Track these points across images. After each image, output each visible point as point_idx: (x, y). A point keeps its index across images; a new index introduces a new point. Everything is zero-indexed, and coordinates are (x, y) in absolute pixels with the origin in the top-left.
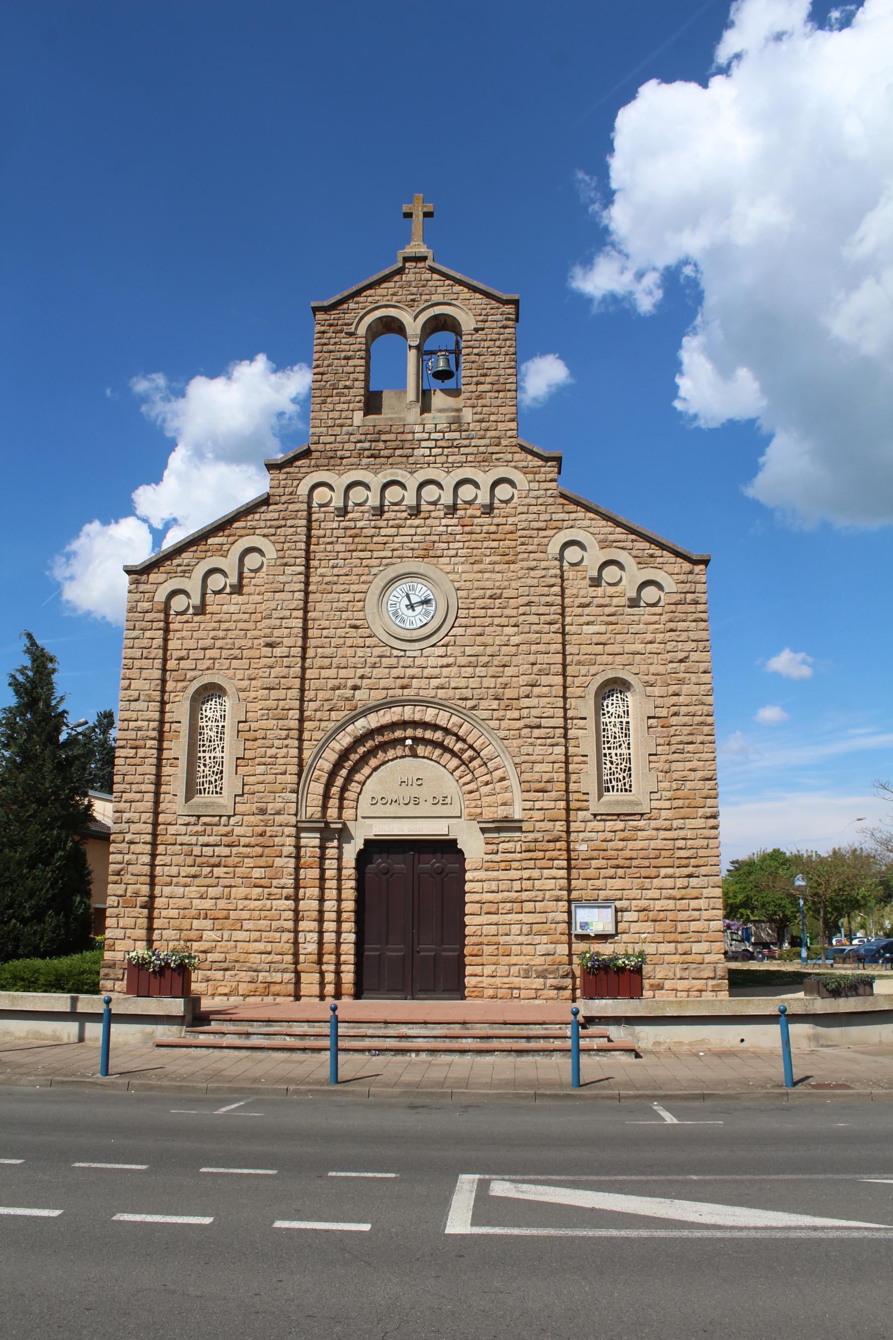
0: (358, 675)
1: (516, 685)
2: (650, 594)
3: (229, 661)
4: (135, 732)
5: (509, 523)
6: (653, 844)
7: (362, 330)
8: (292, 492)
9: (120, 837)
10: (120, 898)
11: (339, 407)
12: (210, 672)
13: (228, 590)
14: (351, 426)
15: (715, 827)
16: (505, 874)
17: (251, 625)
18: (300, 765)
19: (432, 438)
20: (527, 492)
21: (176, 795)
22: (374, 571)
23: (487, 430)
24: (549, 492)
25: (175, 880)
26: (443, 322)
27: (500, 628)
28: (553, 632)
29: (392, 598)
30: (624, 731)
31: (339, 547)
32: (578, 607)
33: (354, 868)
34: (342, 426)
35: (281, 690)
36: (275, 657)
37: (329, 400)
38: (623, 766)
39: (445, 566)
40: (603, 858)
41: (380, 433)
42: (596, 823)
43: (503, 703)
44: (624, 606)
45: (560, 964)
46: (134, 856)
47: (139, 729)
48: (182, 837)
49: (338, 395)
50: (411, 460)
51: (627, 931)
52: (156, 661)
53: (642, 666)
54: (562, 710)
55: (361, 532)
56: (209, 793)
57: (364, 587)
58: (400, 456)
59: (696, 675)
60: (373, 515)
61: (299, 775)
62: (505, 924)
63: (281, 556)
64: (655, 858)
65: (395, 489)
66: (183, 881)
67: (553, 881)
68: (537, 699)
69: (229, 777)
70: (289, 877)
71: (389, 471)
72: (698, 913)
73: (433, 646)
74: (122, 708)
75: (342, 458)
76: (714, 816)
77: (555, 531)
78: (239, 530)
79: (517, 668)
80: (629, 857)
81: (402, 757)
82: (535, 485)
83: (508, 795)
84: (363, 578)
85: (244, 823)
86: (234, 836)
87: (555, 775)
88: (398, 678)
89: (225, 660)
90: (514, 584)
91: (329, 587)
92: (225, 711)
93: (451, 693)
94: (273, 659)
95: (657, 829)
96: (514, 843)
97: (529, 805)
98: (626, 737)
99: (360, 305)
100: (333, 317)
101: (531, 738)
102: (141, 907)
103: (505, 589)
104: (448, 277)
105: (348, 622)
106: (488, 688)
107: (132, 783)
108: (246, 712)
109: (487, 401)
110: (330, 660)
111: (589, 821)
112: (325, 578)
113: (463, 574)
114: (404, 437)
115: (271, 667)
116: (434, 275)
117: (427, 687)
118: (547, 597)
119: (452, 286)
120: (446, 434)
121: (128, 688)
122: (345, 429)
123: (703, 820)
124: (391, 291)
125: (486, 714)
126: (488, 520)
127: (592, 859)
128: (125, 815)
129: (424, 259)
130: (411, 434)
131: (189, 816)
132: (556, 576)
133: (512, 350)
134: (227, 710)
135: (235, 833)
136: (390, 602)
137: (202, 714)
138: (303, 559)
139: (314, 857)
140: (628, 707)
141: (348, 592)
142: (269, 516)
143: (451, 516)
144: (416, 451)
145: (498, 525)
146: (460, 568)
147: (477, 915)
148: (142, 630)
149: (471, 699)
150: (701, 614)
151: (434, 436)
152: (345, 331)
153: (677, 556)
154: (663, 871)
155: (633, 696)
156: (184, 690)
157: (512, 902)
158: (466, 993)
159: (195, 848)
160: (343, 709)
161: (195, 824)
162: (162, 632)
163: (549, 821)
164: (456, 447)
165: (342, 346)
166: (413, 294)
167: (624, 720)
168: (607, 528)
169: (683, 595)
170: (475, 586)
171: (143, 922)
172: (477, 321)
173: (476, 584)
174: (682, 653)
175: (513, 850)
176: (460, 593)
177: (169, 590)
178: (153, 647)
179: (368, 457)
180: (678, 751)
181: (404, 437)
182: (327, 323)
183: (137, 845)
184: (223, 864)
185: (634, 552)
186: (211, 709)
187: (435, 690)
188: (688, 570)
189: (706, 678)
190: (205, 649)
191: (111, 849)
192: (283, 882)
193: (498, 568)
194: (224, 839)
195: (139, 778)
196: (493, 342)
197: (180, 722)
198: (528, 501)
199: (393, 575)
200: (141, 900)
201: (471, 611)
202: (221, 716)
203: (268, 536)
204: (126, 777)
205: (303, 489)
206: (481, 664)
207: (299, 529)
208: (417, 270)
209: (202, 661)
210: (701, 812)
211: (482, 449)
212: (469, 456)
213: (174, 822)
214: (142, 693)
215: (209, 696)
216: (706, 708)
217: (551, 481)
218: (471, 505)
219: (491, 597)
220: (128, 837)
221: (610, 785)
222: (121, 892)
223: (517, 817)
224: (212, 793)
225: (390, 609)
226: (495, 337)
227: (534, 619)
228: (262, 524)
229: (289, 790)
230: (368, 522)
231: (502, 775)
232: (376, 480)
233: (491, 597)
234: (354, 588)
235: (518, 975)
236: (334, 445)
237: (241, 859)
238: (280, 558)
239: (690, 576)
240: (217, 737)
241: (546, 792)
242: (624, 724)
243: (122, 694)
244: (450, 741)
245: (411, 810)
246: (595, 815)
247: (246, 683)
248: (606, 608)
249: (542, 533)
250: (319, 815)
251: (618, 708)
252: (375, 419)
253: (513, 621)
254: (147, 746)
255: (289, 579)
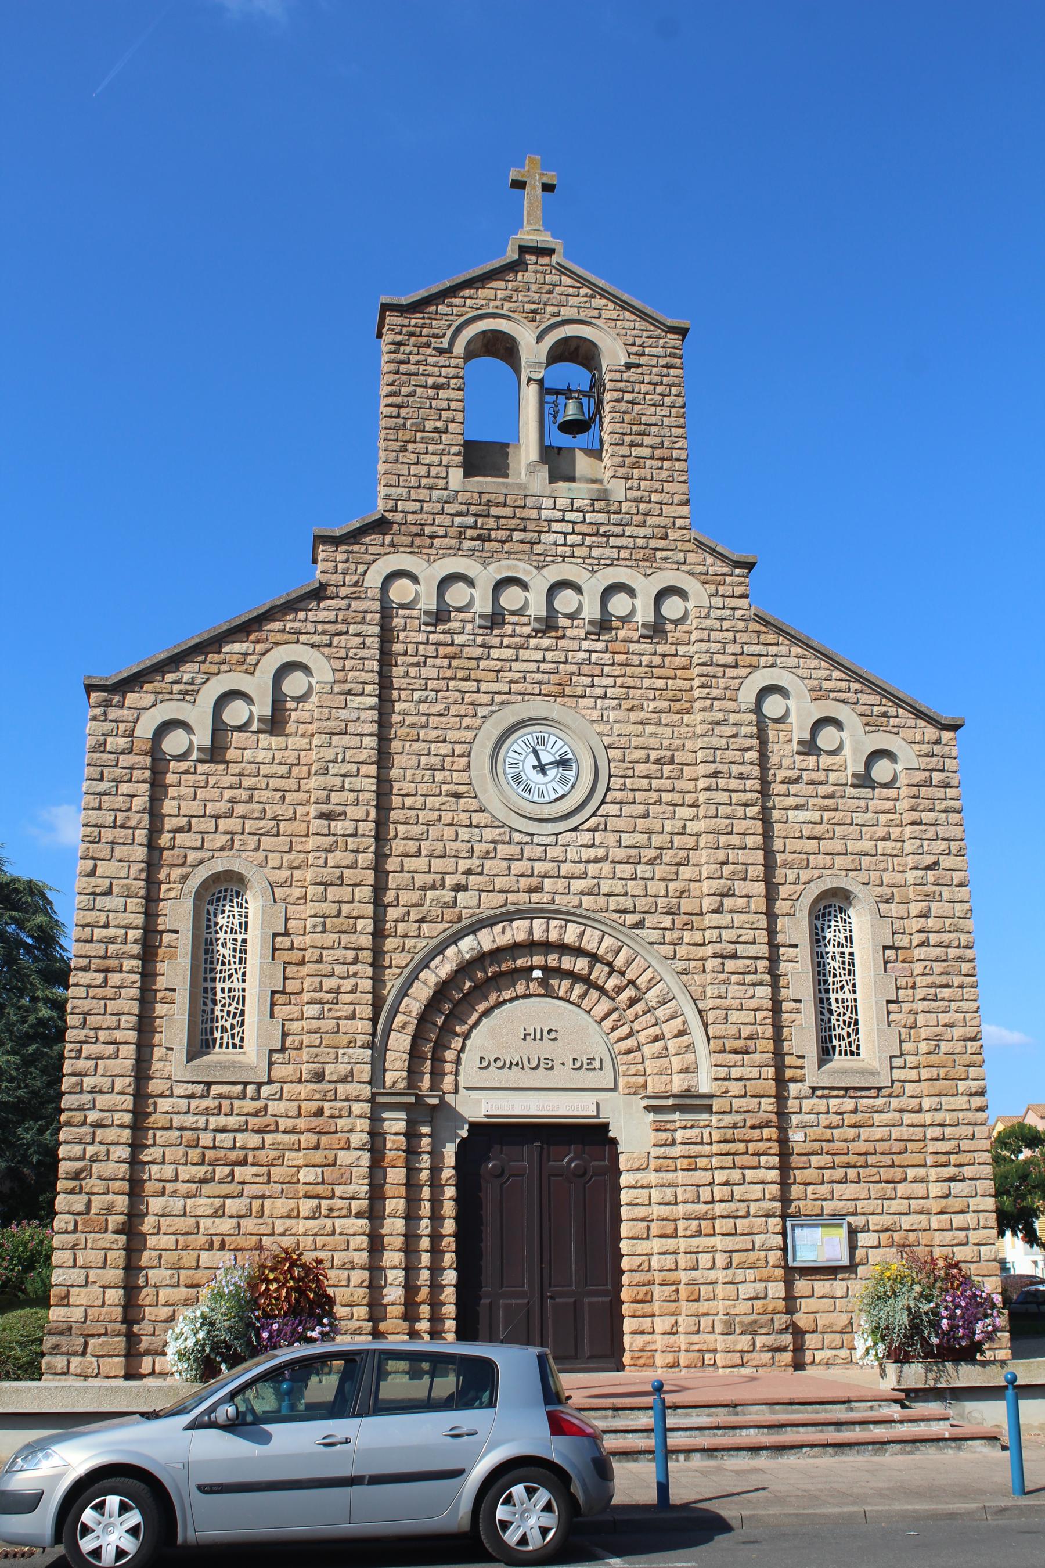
0: (461, 869)
1: (698, 893)
2: (882, 770)
3: (257, 837)
4: (103, 946)
5: (680, 653)
6: (896, 1132)
7: (459, 348)
8: (357, 582)
9: (78, 1117)
10: (78, 1218)
11: (427, 459)
12: (226, 853)
13: (255, 727)
14: (446, 489)
15: (981, 1109)
16: (688, 1176)
17: (292, 784)
18: (377, 1005)
19: (567, 518)
20: (706, 610)
21: (171, 1049)
22: (482, 711)
23: (647, 514)
24: (738, 614)
25: (169, 1187)
26: (572, 348)
27: (671, 808)
28: (750, 818)
29: (511, 754)
30: (847, 967)
31: (426, 672)
32: (782, 782)
33: (454, 1168)
34: (431, 488)
35: (345, 887)
36: (335, 835)
37: (410, 447)
38: (846, 1018)
39: (589, 711)
40: (827, 1153)
41: (488, 503)
42: (815, 1100)
43: (679, 921)
44: (846, 785)
45: (775, 1312)
46: (103, 1149)
47: (112, 940)
48: (182, 1117)
49: (423, 440)
50: (538, 549)
51: (864, 1261)
52: (137, 832)
53: (871, 873)
54: (765, 932)
55: (461, 651)
56: (221, 1046)
57: (469, 735)
58: (522, 542)
59: (950, 888)
60: (480, 627)
61: (375, 1020)
62: (690, 1253)
63: (341, 679)
64: (900, 1153)
65: (514, 590)
66: (182, 1188)
67: (760, 1186)
68: (729, 916)
69: (259, 1021)
70: (361, 1182)
71: (504, 562)
72: (964, 1233)
73: (575, 829)
74: (81, 906)
75: (432, 537)
76: (981, 1093)
77: (749, 670)
78: (273, 634)
79: (697, 869)
80: (863, 1151)
81: (525, 996)
82: (717, 601)
83: (689, 1058)
84: (466, 722)
85: (285, 1095)
86: (268, 1116)
87: (760, 1029)
88: (522, 876)
89: (251, 837)
90: (689, 745)
91: (414, 732)
92: (246, 917)
93: (602, 900)
94: (331, 839)
95: (901, 1111)
96: (699, 1130)
97: (722, 1072)
98: (849, 975)
99: (455, 309)
100: (413, 322)
101: (723, 972)
102: (115, 1232)
103: (677, 750)
104: (585, 282)
105: (445, 788)
106: (655, 896)
107: (99, 1028)
108: (287, 920)
109: (646, 472)
110: (417, 843)
111: (806, 1098)
112: (406, 717)
113: (616, 726)
114: (527, 513)
115: (327, 851)
116: (564, 278)
117: (566, 891)
118: (740, 766)
119: (592, 296)
120: (588, 516)
121: (93, 873)
122: (436, 494)
123: (966, 1098)
124: (500, 294)
125: (655, 936)
126: (649, 648)
127: (813, 1154)
128: (86, 1079)
129: (550, 252)
130: (536, 511)
131: (193, 1082)
132: (751, 737)
133: (680, 401)
134: (250, 915)
135: (269, 1113)
136: (508, 760)
137: (209, 920)
138: (376, 686)
139: (397, 1149)
140: (851, 931)
141: (444, 741)
142: (322, 616)
143: (596, 637)
144: (543, 536)
145: (664, 656)
146: (613, 716)
147: (642, 1239)
148: (114, 780)
149: (634, 912)
150: (953, 802)
151: (569, 516)
152: (433, 345)
153: (918, 717)
154: (911, 1173)
155: (859, 915)
156: (185, 878)
157: (699, 1219)
158: (626, 1359)
159: (202, 1135)
160: (440, 919)
161: (202, 1097)
162: (148, 786)
163: (752, 1096)
164: (602, 535)
165: (429, 368)
166: (534, 303)
167: (847, 951)
168: (818, 668)
169: (927, 774)
170: (633, 744)
171: (117, 1256)
172: (629, 354)
173: (635, 741)
174: (929, 856)
175: (699, 1140)
176: (613, 753)
177: (159, 720)
178: (134, 809)
179: (473, 539)
180: (929, 997)
181: (527, 513)
182: (405, 330)
183: (108, 1130)
184: (250, 1159)
185: (860, 709)
186: (223, 912)
187: (578, 897)
188: (934, 738)
189: (962, 893)
190: (217, 817)
191: (62, 1137)
192: (351, 1189)
193: (665, 718)
194: (254, 1121)
195: (111, 1021)
196: (652, 387)
197: (177, 932)
198: (708, 623)
199: (513, 720)
200: (114, 1221)
201: (628, 780)
202: (240, 923)
203: (319, 646)
204: (88, 1017)
205: (374, 578)
206: (645, 860)
207: (369, 641)
208: (540, 268)
209: (211, 836)
210: (962, 1086)
211: (640, 542)
212: (622, 551)
213: (168, 1093)
214: (115, 882)
215: (220, 892)
216: (963, 938)
217: (741, 596)
218: (624, 622)
219: (657, 762)
220: (92, 1117)
221: (829, 1045)
222: (80, 1207)
223: (704, 1089)
224: (227, 1047)
225: (508, 771)
226: (657, 379)
227: (723, 797)
228: (310, 627)
229: (359, 1043)
230: (471, 637)
231: (681, 1028)
232: (486, 575)
233: (657, 762)
234: (452, 735)
235: (710, 1329)
236: (420, 516)
237: (279, 1153)
238: (339, 681)
239: (935, 747)
240: (234, 957)
241: (747, 1053)
242: (847, 956)
243: (80, 883)
244: (599, 973)
245: (540, 1078)
246: (814, 1089)
247: (285, 874)
248: (820, 787)
249: (730, 673)
250: (402, 1085)
251: (837, 933)
252: (482, 482)
253: (689, 799)
254: (125, 968)
255: (354, 715)
